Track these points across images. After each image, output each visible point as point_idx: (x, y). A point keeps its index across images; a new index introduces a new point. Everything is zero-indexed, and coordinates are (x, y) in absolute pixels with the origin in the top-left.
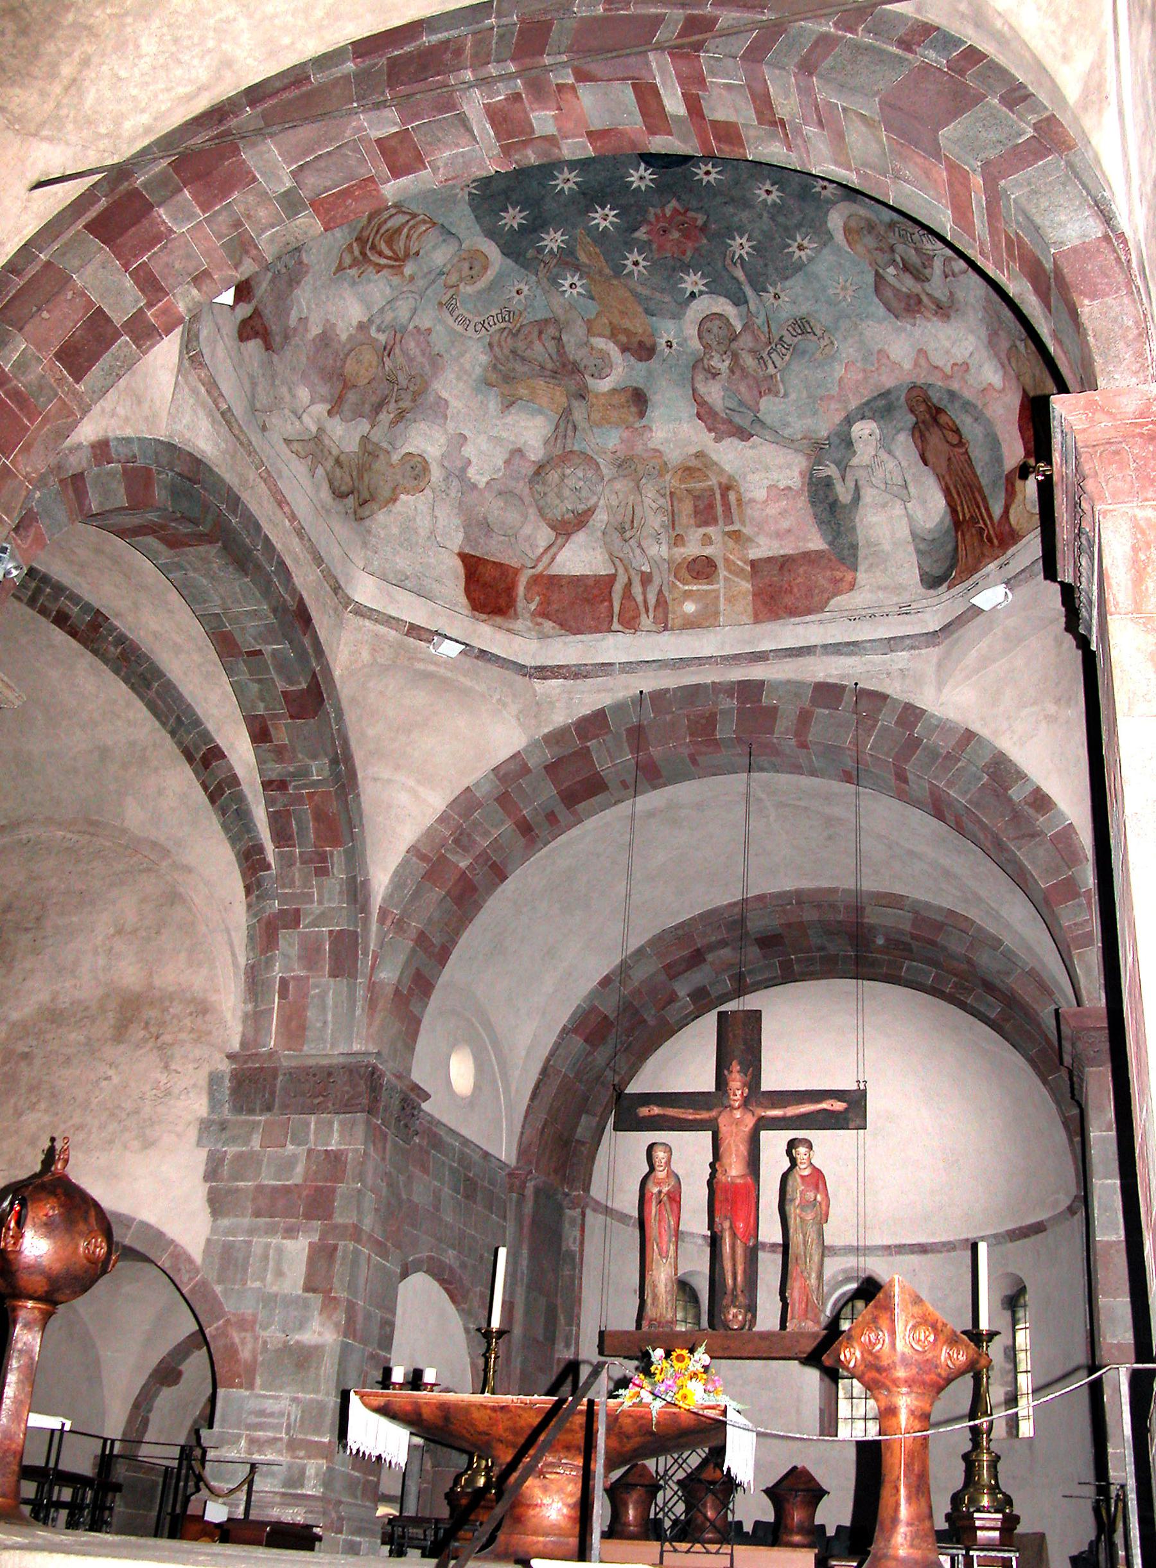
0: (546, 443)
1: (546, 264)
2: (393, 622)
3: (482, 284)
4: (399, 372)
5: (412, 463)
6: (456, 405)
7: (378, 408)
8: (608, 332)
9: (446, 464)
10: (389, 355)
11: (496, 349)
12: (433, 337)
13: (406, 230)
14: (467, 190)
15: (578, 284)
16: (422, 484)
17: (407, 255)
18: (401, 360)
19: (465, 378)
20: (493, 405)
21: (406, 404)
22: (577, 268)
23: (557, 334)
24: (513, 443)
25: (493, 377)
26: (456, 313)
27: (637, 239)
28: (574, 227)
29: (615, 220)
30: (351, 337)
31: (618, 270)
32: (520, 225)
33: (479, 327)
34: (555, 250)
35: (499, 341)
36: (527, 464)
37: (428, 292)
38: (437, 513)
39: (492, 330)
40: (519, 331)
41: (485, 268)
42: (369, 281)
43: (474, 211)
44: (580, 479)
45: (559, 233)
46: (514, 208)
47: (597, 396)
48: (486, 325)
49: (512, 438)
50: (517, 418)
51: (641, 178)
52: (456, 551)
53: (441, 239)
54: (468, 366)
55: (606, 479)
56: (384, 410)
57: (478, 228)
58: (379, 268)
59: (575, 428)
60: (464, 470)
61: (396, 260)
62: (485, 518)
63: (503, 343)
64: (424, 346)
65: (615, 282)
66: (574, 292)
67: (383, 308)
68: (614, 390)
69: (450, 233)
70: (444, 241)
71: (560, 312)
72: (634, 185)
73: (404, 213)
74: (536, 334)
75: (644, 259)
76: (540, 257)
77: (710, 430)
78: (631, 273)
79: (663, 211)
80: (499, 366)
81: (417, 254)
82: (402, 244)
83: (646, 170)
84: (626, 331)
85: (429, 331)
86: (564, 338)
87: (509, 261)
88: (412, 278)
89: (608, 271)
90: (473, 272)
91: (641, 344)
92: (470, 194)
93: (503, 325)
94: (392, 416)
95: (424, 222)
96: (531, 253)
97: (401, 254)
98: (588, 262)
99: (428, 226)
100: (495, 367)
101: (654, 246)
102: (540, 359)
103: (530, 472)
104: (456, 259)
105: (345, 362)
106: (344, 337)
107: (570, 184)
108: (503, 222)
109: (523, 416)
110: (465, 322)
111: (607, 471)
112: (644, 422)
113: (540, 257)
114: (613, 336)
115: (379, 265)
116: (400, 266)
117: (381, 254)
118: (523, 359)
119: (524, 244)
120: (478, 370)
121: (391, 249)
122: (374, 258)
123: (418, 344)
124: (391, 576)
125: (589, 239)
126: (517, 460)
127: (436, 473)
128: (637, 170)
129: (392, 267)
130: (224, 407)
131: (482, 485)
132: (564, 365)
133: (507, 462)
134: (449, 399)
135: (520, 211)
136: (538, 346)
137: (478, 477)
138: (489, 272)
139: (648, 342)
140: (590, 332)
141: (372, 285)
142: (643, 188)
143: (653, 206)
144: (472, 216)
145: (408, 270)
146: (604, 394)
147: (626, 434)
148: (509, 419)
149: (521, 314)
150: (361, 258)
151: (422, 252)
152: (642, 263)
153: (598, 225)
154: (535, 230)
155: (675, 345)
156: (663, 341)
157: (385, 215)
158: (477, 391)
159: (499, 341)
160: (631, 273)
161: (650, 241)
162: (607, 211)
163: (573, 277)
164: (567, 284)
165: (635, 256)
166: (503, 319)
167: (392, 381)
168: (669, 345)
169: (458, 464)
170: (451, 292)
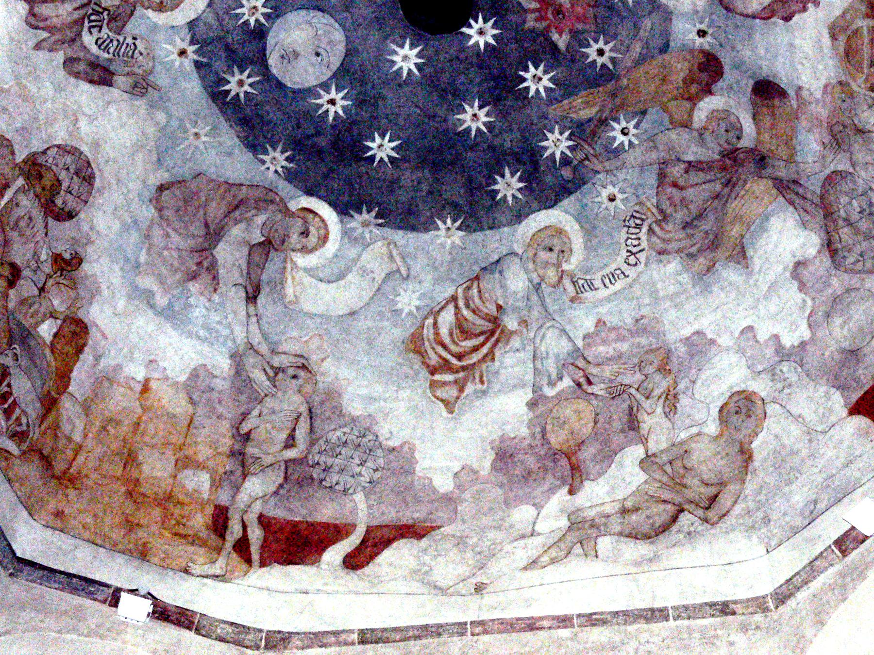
0: (804, 225)
1: (587, 159)
2: (817, 563)
3: (577, 241)
4: (619, 379)
5: (733, 411)
6: (706, 323)
7: (632, 424)
8: (687, 105)
9: (760, 368)
10: (590, 383)
11: (669, 247)
12: (612, 320)
13: (465, 312)
14: (453, 230)
15: (624, 124)
16: (759, 412)
17: (495, 321)
18: (607, 371)
19: (683, 298)
20: (730, 274)
21: (662, 384)
22: (603, 122)
23: (683, 166)
24: (785, 269)
25: (702, 261)
26: (597, 283)
27: (568, 45)
28: (545, 116)
29: (541, 68)
30: (531, 425)
31: (605, 76)
32: (520, 180)
33: (632, 260)
34: (571, 143)
35: (664, 241)
36: (817, 261)
37: (551, 310)
38: (796, 411)
39: (644, 244)
40: (661, 211)
41: (560, 232)
42: (497, 373)
43: (481, 229)
44: (850, 203)
45: (549, 135)
46: (495, 182)
47: (759, 142)
48: (634, 250)
49: (780, 269)
50: (760, 252)
51: (481, 32)
52: (844, 413)
53: (497, 275)
54: (672, 289)
55: (851, 170)
56: (642, 416)
57: (506, 229)
58: (490, 356)
59: (795, 182)
60: (779, 349)
61: (493, 332)
62: (843, 351)
63: (668, 236)
64: (613, 335)
65: (625, 82)
66: (633, 131)
67: (535, 369)
68: (754, 118)
69: (497, 262)
70: (501, 272)
71: (654, 156)
72: (491, 41)
73: (442, 308)
74: (674, 191)
75: (596, 41)
76: (575, 162)
77: (804, 9)
78: (613, 60)
79: (532, 11)
80: (694, 250)
81: (499, 307)
82: (479, 322)
83: (470, 26)
84: (688, 81)
85: (600, 323)
86: (690, 158)
87: (566, 202)
88: (524, 322)
89: (610, 86)
90: (557, 249)
91: (702, 68)
92: (459, 228)
93: (645, 229)
94: (659, 410)
95: (468, 288)
96: (567, 173)
97: (488, 326)
98: (597, 109)
99: (475, 284)
100: (691, 256)
101: (580, 26)
102: (706, 195)
103: (827, 261)
104: (531, 266)
105: (549, 443)
106: (524, 431)
107: (482, 114)
108: (510, 199)
109: (762, 241)
110: (613, 277)
111: (843, 165)
112: (791, 93)
113: (575, 162)
114: (693, 100)
115: (487, 355)
116: (502, 332)
117: (476, 349)
118: (700, 216)
119: (549, 179)
120: (685, 278)
121: (477, 335)
122: (475, 358)
123: (604, 342)
124: (799, 522)
125: (566, 102)
126: (806, 273)
127: (761, 387)
128: (470, 37)
129: (497, 341)
130: (355, 637)
131: (806, 334)
132: (724, 169)
133: (802, 287)
134: (696, 327)
135: (503, 176)
136: (690, 193)
137: (797, 333)
138: (567, 228)
139: (701, 59)
140: (686, 125)
141: (502, 371)
142: (495, 32)
143: (524, 21)
144: (488, 232)
145: (511, 323)
146: (758, 133)
147: (804, 123)
148: (757, 263)
149: (641, 203)
150: (461, 375)
151: (501, 302)
152: (601, 44)
153: (546, 89)
154: (536, 165)
155: (703, 27)
156: (699, 41)
157: (428, 332)
158: (707, 289)
159: (664, 241)
160: (613, 60)
161: (571, 31)
162: (528, 76)
163: (614, 129)
164: (620, 138)
165: (592, 52)
166: (638, 226)
167: (617, 392)
168: (702, 33)
169: (769, 352)
170: (567, 282)
